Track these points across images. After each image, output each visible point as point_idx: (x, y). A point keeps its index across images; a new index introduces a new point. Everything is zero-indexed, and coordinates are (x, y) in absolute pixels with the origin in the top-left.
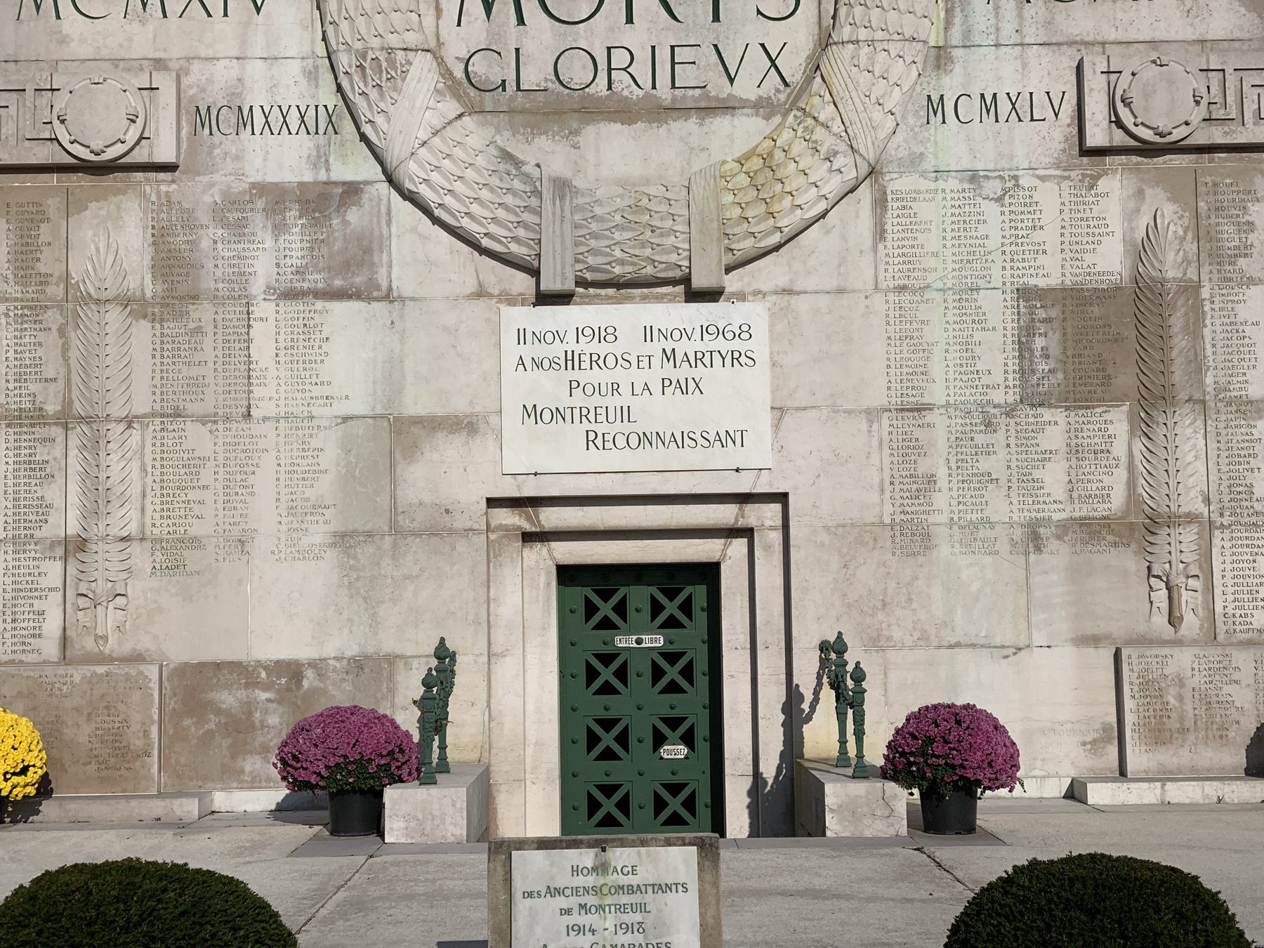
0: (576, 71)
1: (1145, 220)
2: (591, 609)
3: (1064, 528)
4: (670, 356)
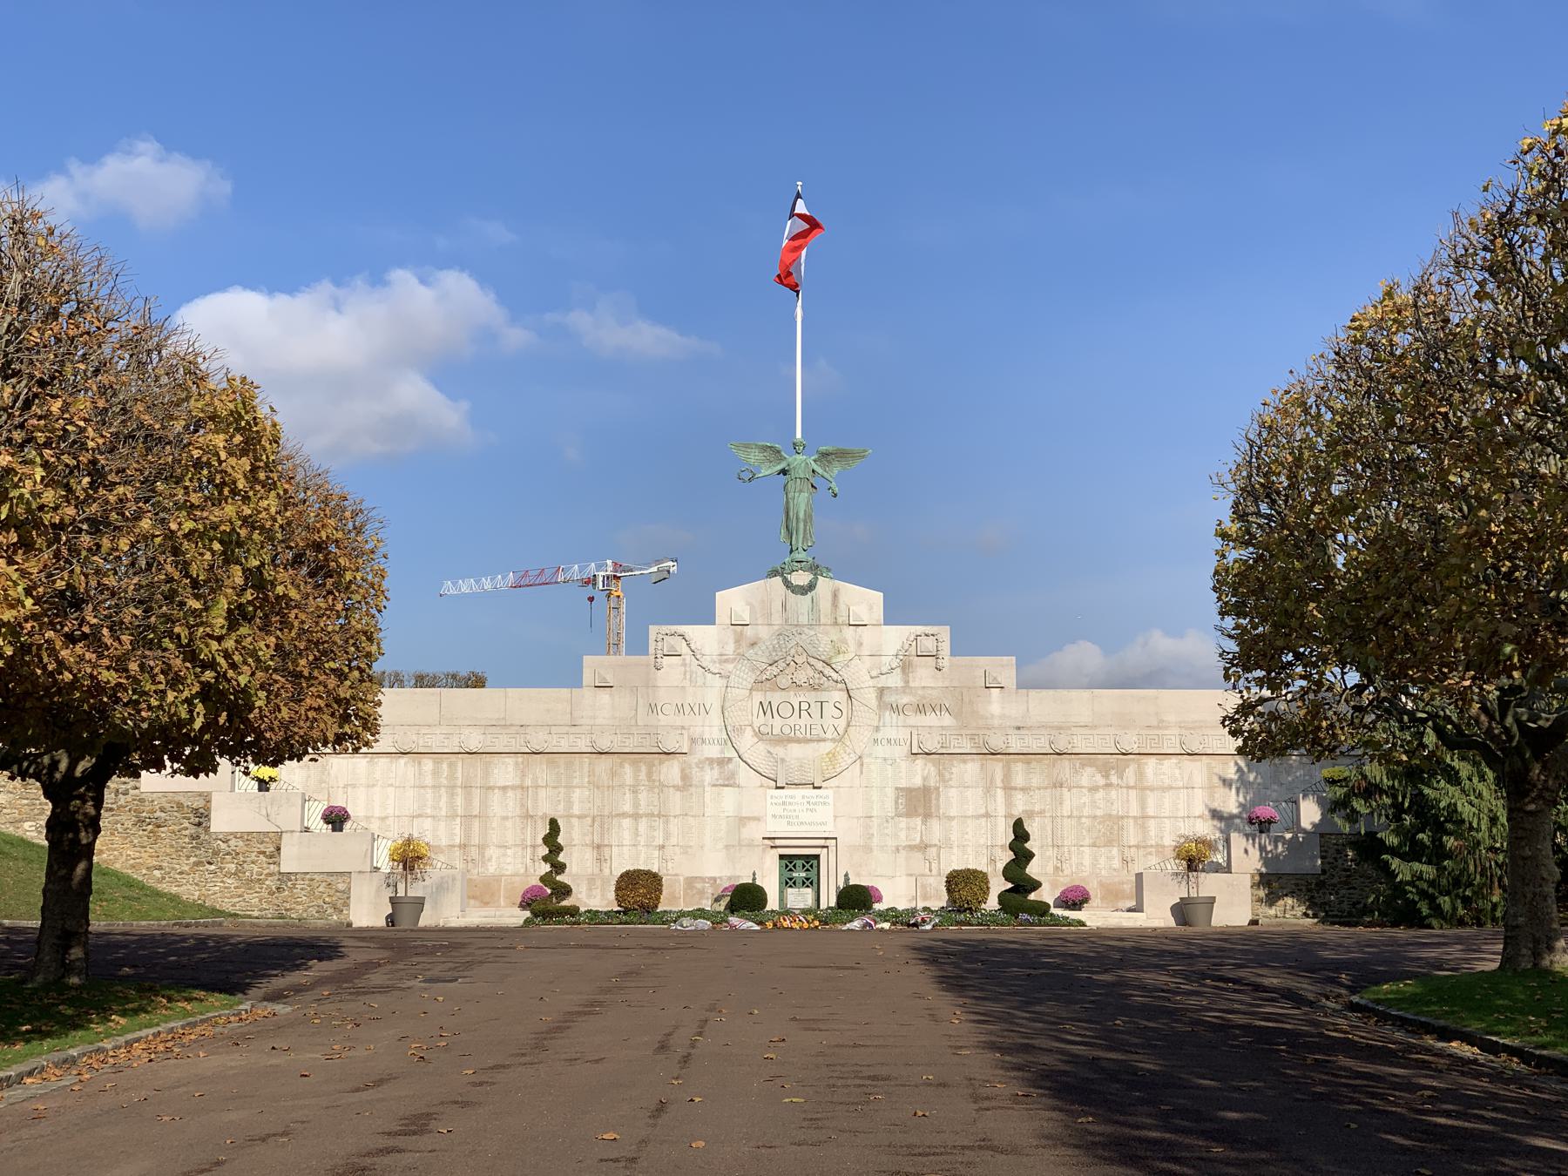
0: (787, 730)
1: (926, 771)
2: (787, 866)
3: (904, 848)
4: (808, 803)
